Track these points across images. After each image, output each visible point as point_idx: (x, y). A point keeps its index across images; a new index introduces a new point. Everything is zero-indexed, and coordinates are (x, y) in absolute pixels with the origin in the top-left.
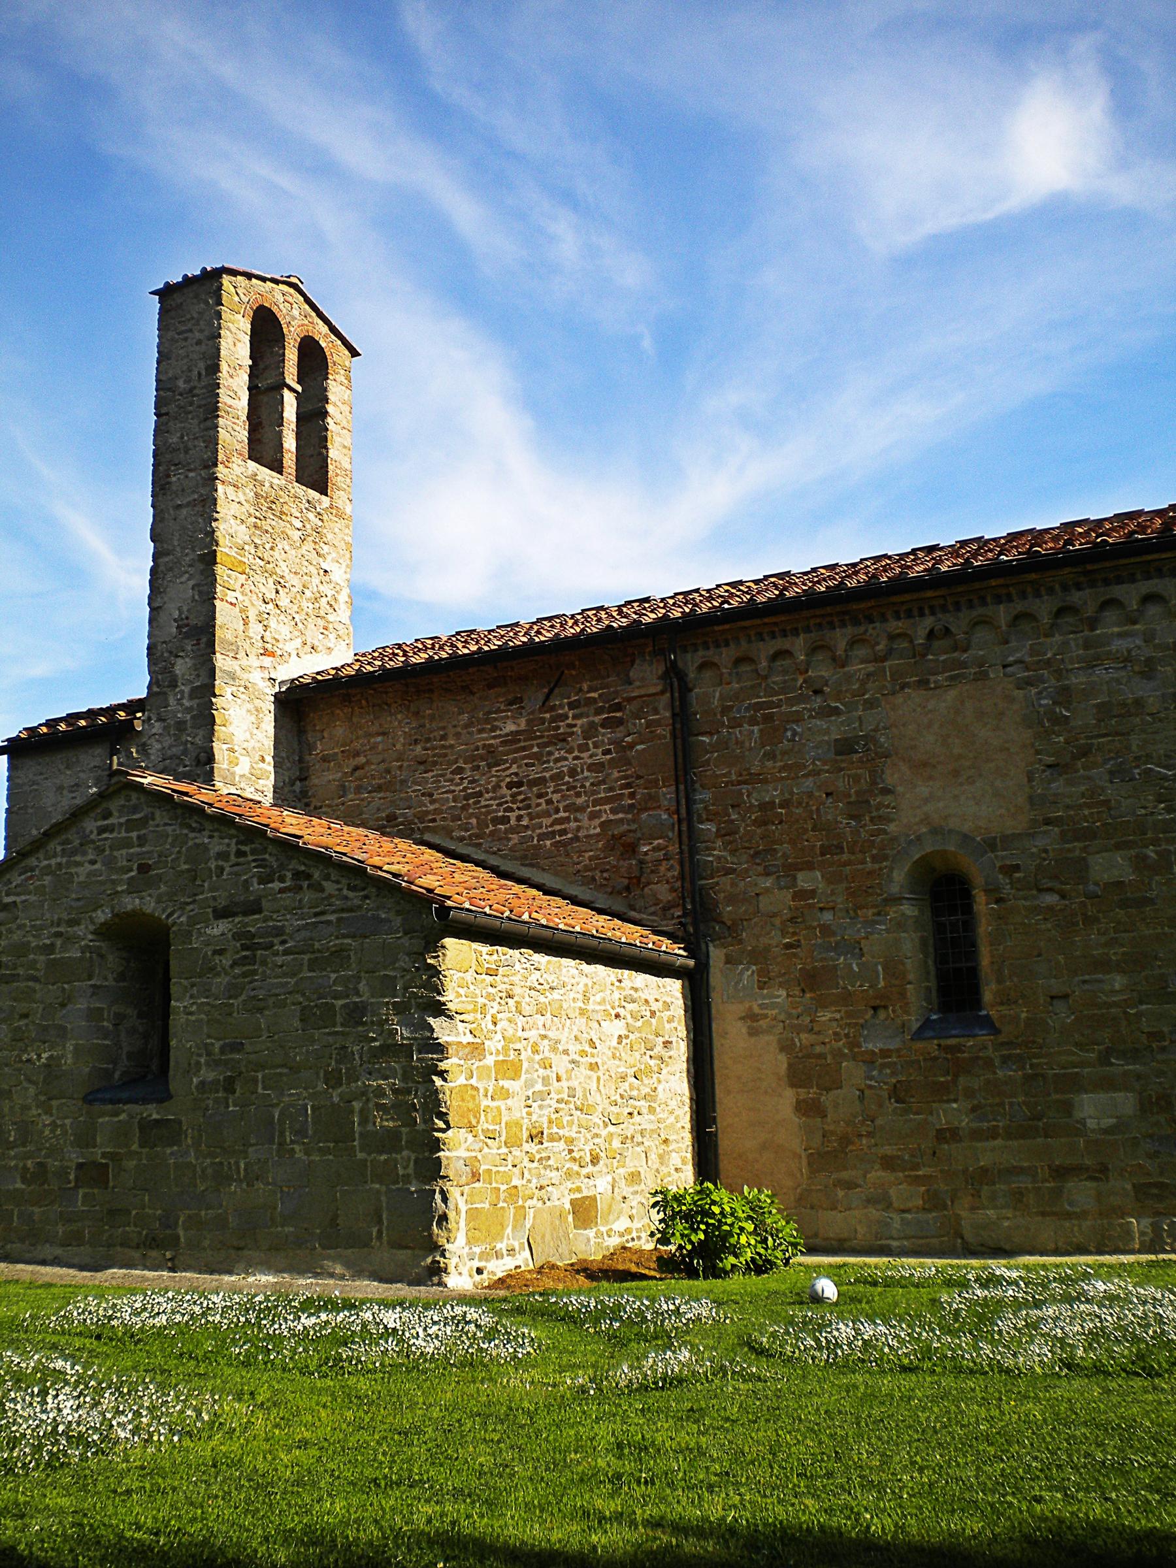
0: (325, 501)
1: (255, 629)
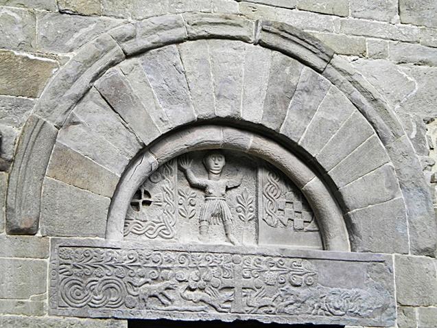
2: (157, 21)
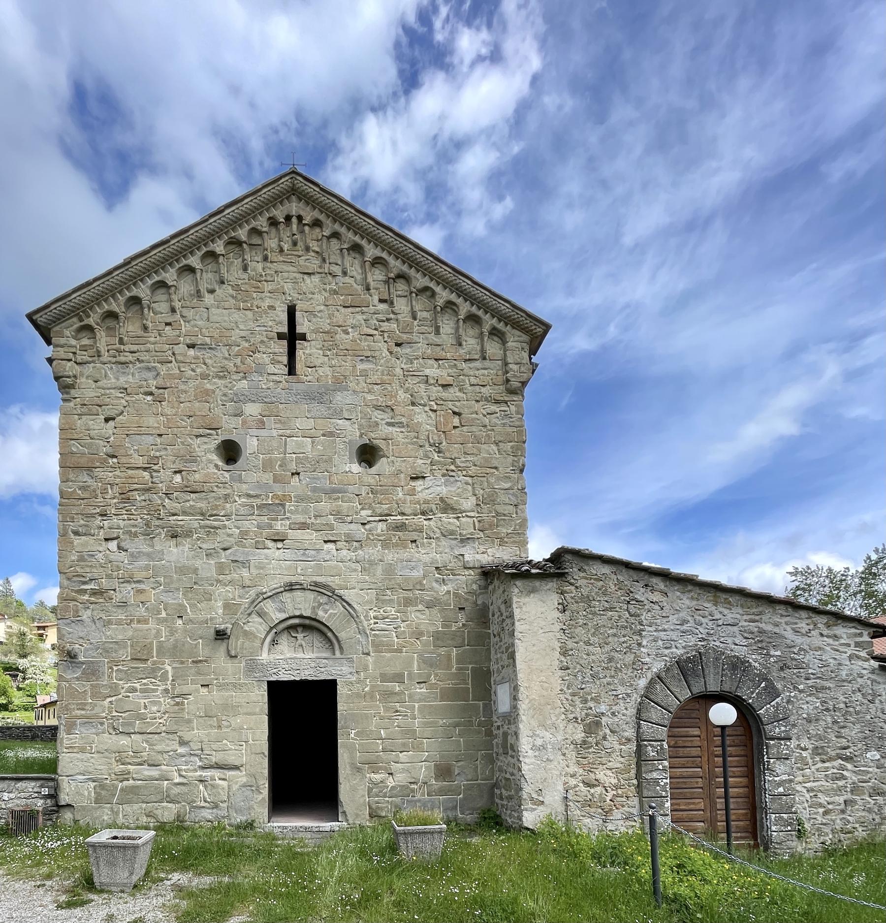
2: (275, 586)
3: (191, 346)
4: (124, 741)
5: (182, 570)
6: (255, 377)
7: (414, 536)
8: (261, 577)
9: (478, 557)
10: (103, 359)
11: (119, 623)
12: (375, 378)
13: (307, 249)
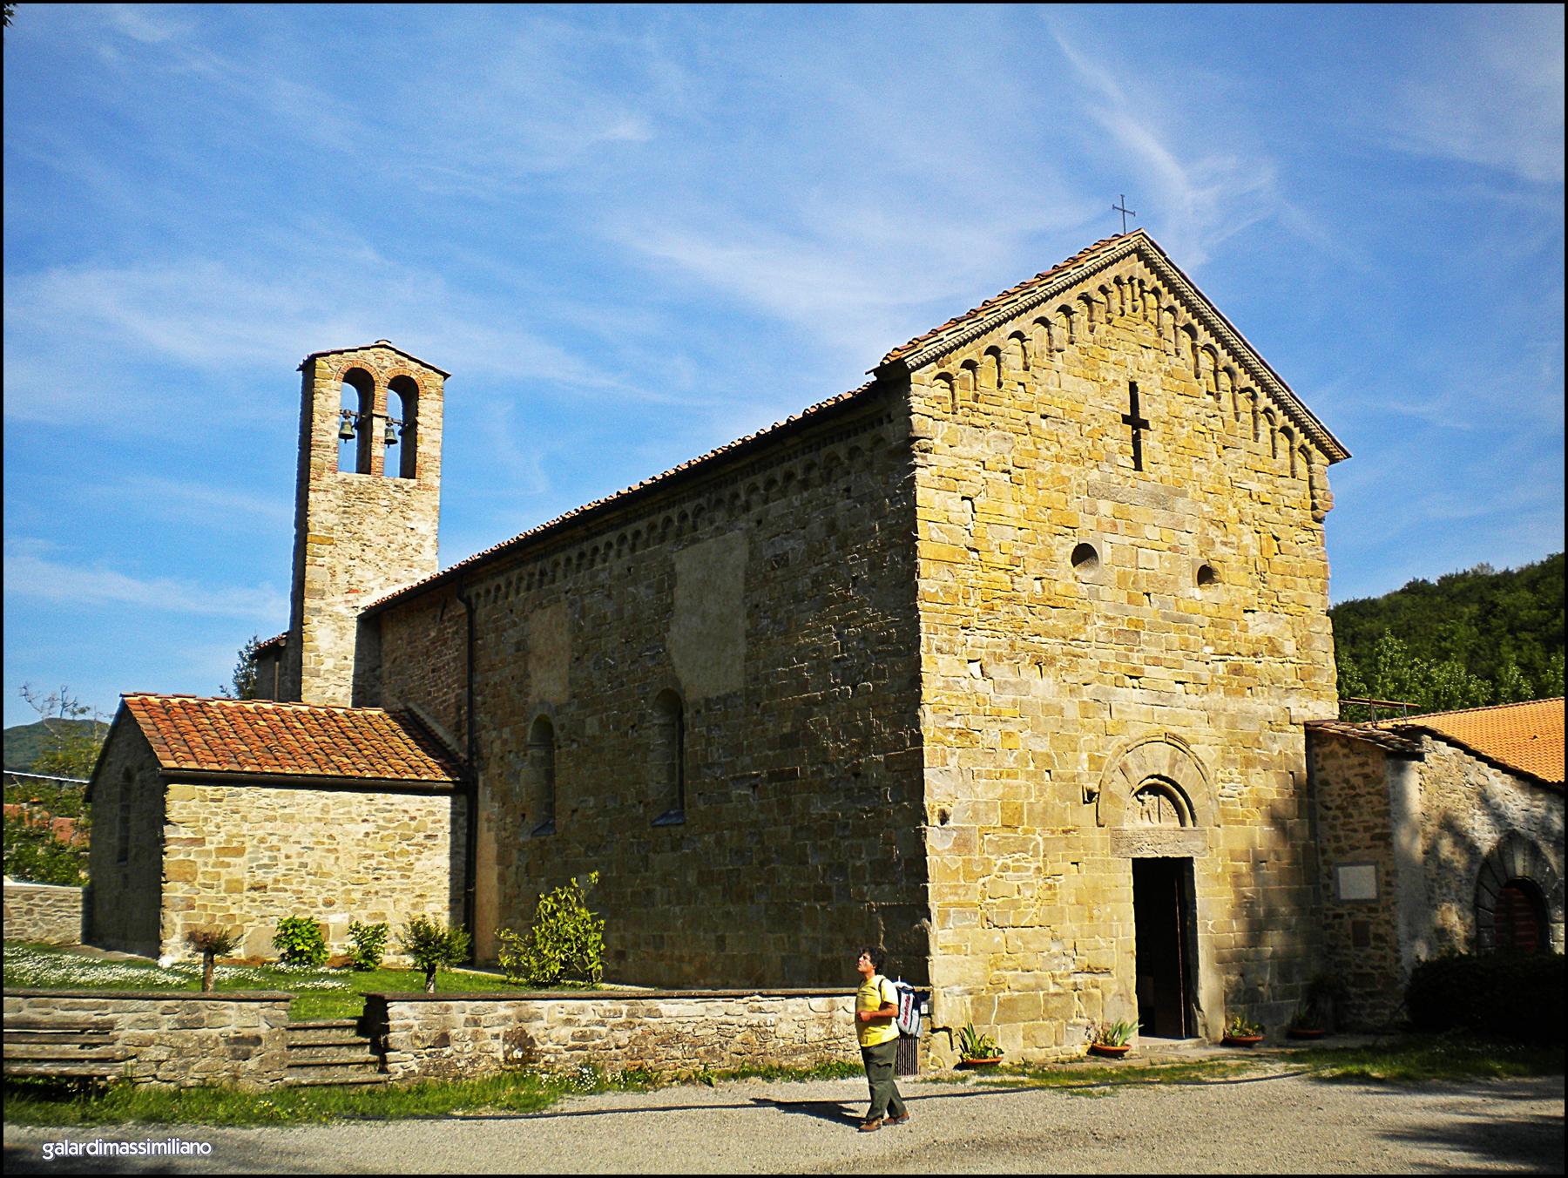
0: (413, 482)
1: (342, 579)
3: (1044, 417)
4: (998, 936)
5: (1048, 708)
6: (1106, 467)
7: (1249, 681)
8: (1124, 724)
9: (1302, 711)
10: (959, 417)
11: (989, 775)
12: (1207, 486)
13: (1145, 318)
